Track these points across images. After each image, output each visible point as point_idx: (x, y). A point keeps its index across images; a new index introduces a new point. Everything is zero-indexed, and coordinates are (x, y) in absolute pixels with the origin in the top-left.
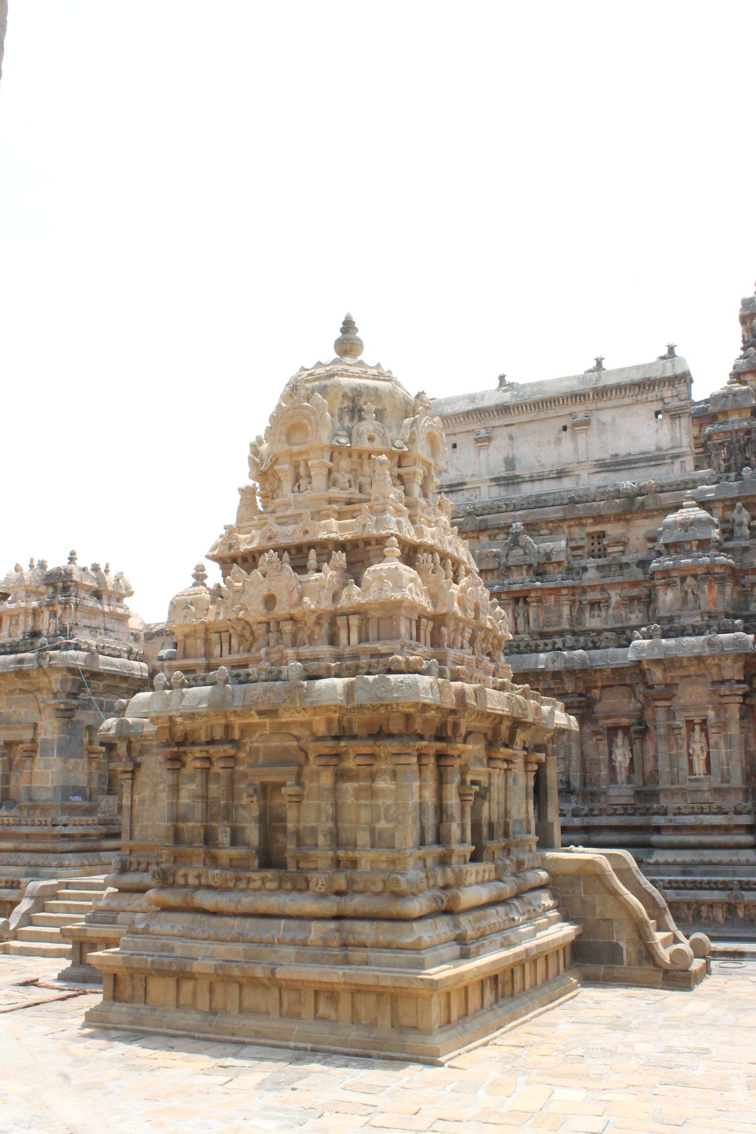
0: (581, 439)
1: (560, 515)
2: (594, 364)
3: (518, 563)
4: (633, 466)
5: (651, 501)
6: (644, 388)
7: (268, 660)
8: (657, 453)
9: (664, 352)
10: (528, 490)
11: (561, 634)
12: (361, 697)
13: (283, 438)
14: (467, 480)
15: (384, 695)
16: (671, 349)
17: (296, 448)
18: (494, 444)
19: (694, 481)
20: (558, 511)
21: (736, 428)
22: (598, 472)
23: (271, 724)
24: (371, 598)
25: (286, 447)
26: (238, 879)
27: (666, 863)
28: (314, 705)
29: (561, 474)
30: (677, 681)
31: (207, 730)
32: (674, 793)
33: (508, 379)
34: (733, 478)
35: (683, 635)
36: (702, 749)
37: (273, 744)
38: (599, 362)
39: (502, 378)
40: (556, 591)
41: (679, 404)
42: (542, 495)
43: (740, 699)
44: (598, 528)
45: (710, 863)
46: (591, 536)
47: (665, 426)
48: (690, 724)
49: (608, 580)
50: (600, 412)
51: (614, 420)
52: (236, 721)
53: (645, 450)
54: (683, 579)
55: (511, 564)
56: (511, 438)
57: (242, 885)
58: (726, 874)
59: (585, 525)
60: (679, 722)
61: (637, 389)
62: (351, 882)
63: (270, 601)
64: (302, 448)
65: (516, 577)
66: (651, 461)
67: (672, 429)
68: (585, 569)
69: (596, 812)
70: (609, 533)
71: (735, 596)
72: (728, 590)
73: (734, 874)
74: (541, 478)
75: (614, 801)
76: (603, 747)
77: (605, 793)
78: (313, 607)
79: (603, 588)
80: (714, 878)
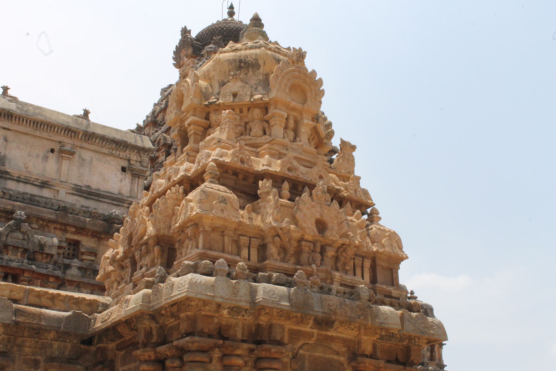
0: (65, 164)
1: (53, 217)
2: (82, 113)
3: (16, 245)
4: (101, 199)
6: (119, 146)
20: (51, 214)
22: (73, 194)
23: (318, 334)
28: (383, 326)
29: (44, 185)
31: (243, 329)
33: (10, 92)
37: (317, 354)
38: (86, 113)
41: (141, 168)
42: (36, 196)
44: (76, 237)
47: (127, 180)
50: (82, 150)
51: (91, 160)
53: (111, 191)
56: (6, 140)
59: (66, 231)
61: (114, 145)
66: (114, 200)
74: (26, 182)
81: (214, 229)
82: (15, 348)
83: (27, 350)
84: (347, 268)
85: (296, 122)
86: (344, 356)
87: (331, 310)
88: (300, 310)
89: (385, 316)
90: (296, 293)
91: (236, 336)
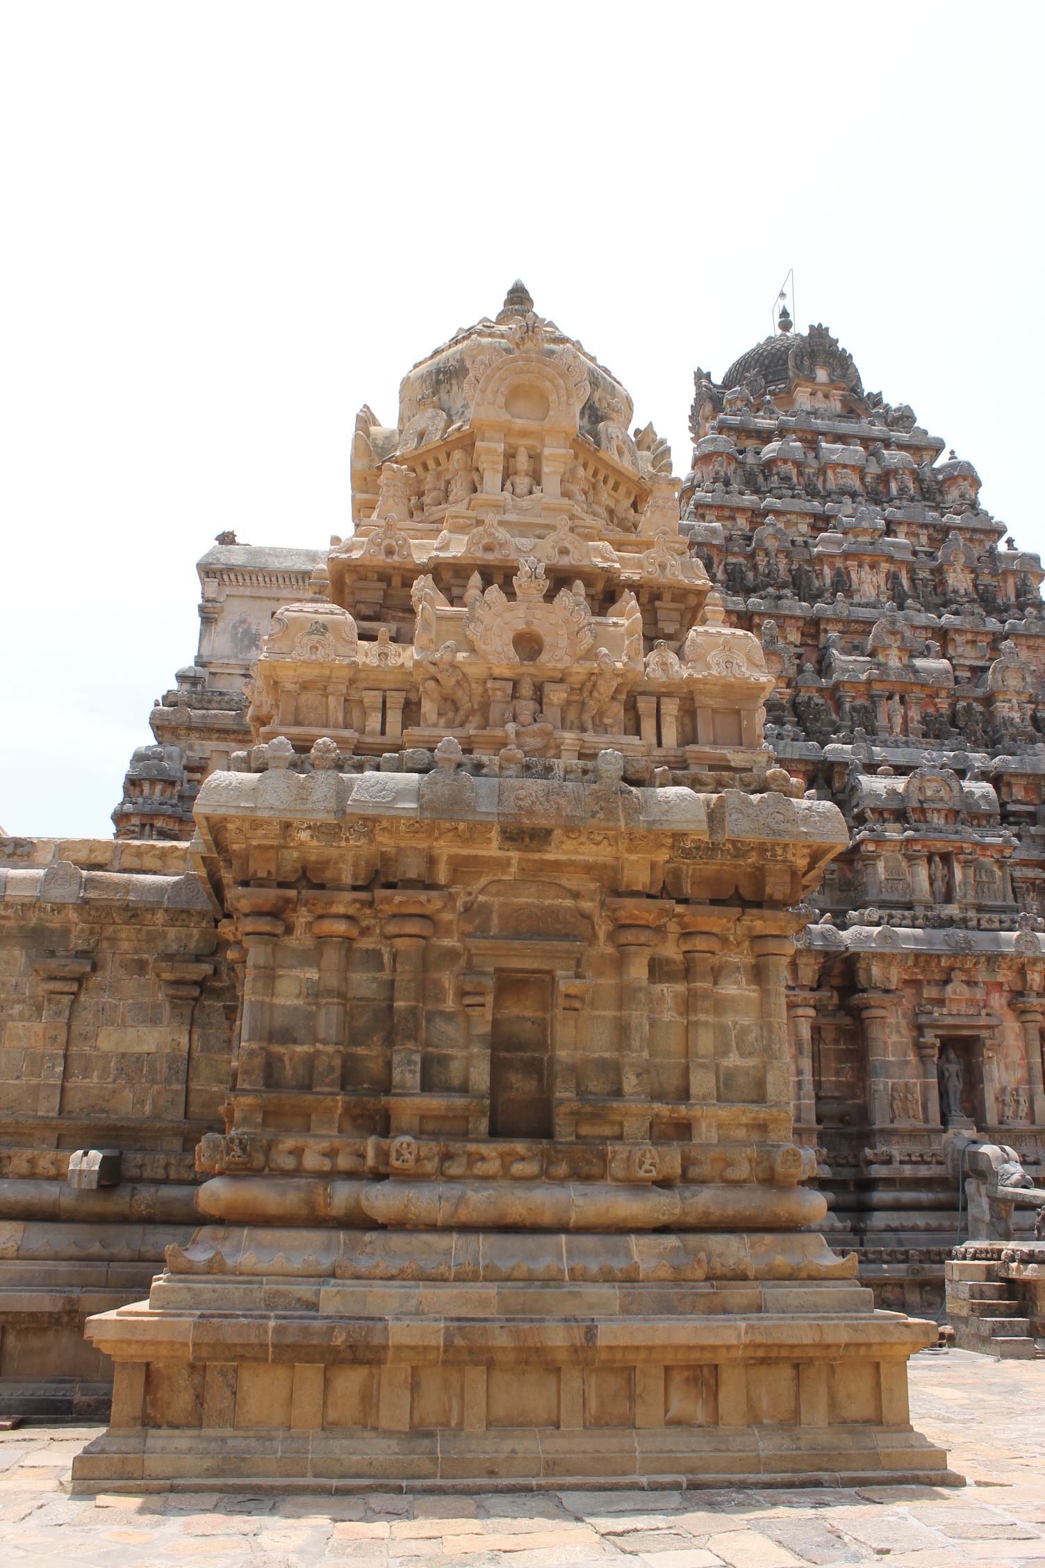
7: (519, 747)
12: (737, 827)
13: (501, 400)
15: (782, 827)
17: (519, 423)
23: (521, 860)
24: (714, 673)
25: (505, 416)
26: (447, 1157)
28: (657, 827)
31: (356, 865)
37: (523, 900)
52: (445, 849)
57: (455, 1169)
62: (687, 1162)
63: (528, 645)
64: (534, 425)
78: (619, 665)
81: (305, 686)
82: (105, 944)
83: (125, 945)
84: (607, 721)
85: (535, 458)
86: (592, 900)
87: (520, 808)
88: (439, 814)
89: (666, 807)
90: (433, 782)
91: (339, 879)
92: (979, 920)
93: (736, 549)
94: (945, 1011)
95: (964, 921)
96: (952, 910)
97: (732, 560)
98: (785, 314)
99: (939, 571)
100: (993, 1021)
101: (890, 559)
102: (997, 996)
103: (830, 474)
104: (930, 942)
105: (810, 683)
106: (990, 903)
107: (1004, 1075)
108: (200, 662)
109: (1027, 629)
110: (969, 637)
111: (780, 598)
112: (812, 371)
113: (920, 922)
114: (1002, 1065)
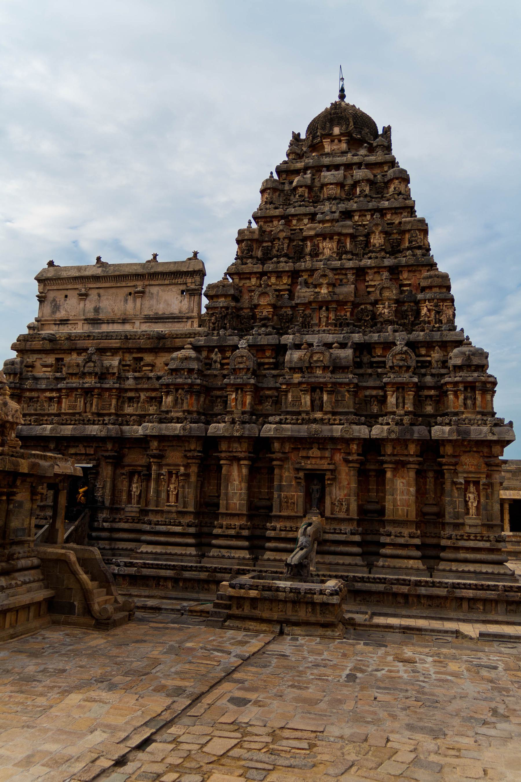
2: (152, 257)
5: (169, 343)
8: (180, 315)
9: (191, 255)
10: (105, 328)
11: (110, 415)
14: (71, 318)
16: (196, 254)
18: (88, 298)
19: (195, 334)
20: (117, 343)
21: (221, 305)
22: (146, 322)
27: (147, 553)
29: (124, 321)
30: (166, 448)
32: (157, 512)
34: (215, 334)
35: (171, 422)
36: (175, 488)
38: (155, 256)
39: (99, 259)
40: (109, 389)
42: (110, 332)
43: (200, 462)
44: (139, 355)
45: (170, 554)
46: (135, 359)
48: (170, 474)
49: (139, 386)
50: (151, 287)
51: (158, 293)
54: (177, 390)
55: (86, 371)
56: (99, 295)
58: (177, 561)
59: (132, 353)
60: (164, 471)
65: (88, 380)
67: (189, 302)
68: (128, 378)
69: (117, 520)
70: (145, 358)
71: (207, 402)
72: (202, 399)
73: (182, 561)
74: (113, 322)
75: (128, 514)
76: (126, 483)
77: (123, 509)
79: (137, 390)
80: (169, 563)
92: (329, 419)
93: (267, 239)
94: (309, 462)
95: (322, 419)
96: (319, 415)
97: (265, 244)
98: (342, 90)
99: (368, 236)
100: (331, 467)
101: (339, 234)
102: (338, 455)
103: (325, 189)
104: (299, 432)
105: (286, 304)
106: (341, 410)
107: (338, 492)
108: (37, 320)
109: (406, 262)
110: (376, 270)
111: (279, 262)
112: (331, 129)
113: (299, 421)
114: (337, 487)
